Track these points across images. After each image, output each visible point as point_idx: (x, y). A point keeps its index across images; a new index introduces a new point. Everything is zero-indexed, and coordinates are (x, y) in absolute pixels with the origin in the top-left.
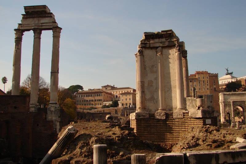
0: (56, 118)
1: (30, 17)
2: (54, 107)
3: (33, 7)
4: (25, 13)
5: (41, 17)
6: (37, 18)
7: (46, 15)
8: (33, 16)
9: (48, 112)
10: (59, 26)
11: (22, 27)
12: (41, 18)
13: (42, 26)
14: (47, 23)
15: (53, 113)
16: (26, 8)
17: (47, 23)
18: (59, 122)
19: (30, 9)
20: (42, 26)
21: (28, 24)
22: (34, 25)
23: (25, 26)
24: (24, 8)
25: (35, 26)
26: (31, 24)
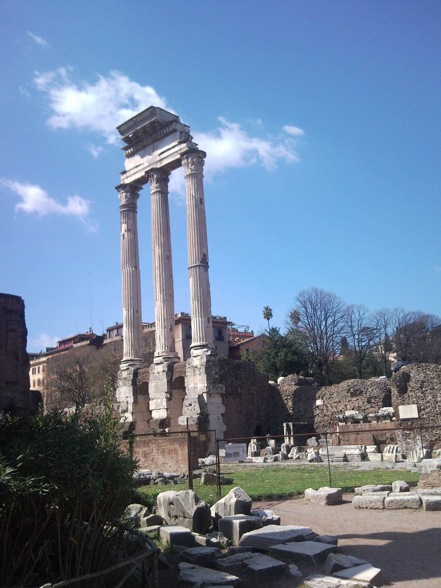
0: (203, 385)
1: (138, 148)
2: (199, 358)
3: (131, 123)
4: (126, 145)
5: (157, 140)
6: (151, 146)
7: (165, 132)
8: (142, 144)
9: (187, 370)
10: (200, 149)
11: (127, 177)
12: (157, 143)
15: (197, 372)
16: (122, 129)
18: (222, 395)
19: (129, 129)
20: (161, 160)
21: (137, 167)
22: (146, 164)
23: (132, 172)
24: (119, 131)
25: (148, 167)
26: (141, 165)
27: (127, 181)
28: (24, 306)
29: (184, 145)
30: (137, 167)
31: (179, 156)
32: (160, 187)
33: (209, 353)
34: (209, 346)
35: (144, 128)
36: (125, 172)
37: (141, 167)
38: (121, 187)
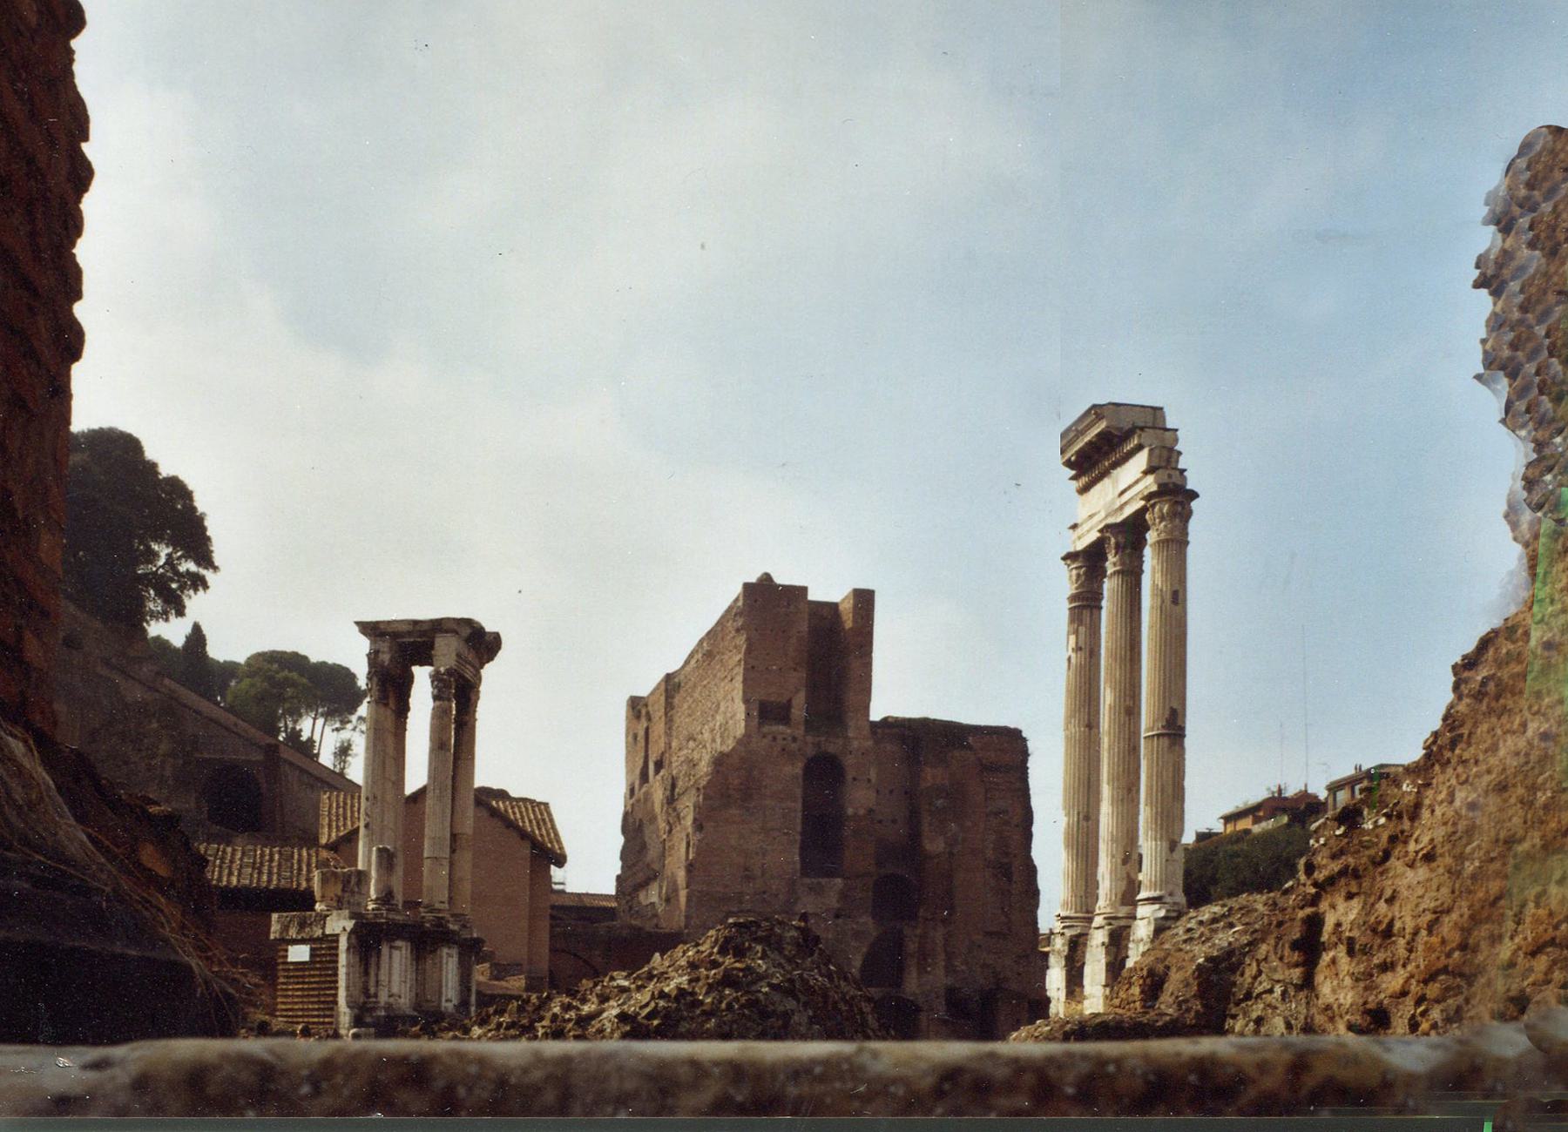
13: (1122, 507)
14: (1130, 487)
17: (1130, 487)
20: (1122, 507)
21: (1091, 517)
22: (1103, 514)
27: (1080, 546)
28: (1025, 754)
29: (1150, 479)
30: (1091, 517)
31: (1143, 503)
32: (1123, 564)
33: (1162, 913)
34: (1168, 899)
35: (1090, 443)
36: (1074, 527)
37: (1096, 519)
38: (1070, 557)
